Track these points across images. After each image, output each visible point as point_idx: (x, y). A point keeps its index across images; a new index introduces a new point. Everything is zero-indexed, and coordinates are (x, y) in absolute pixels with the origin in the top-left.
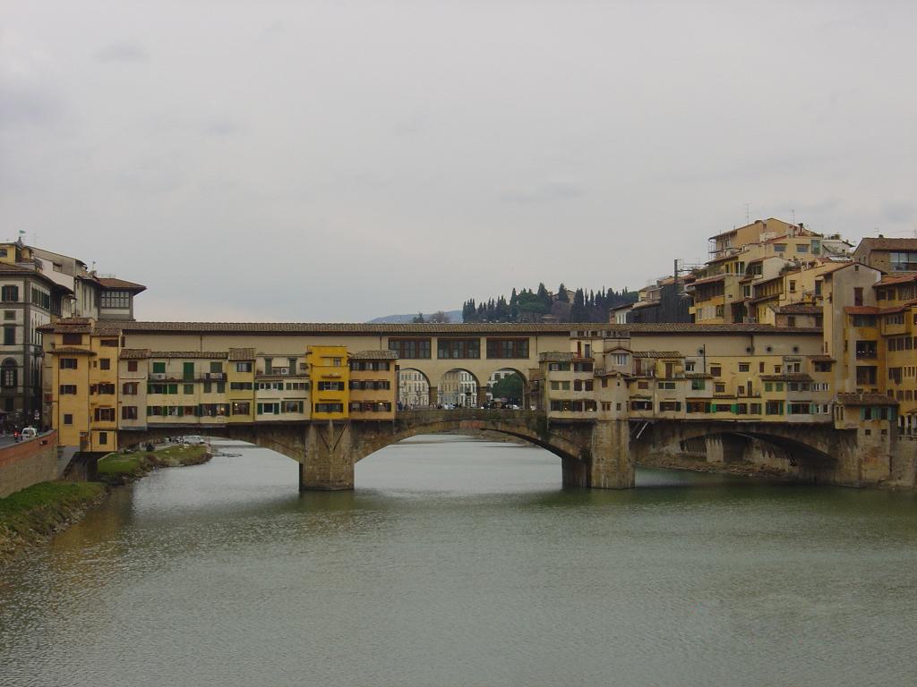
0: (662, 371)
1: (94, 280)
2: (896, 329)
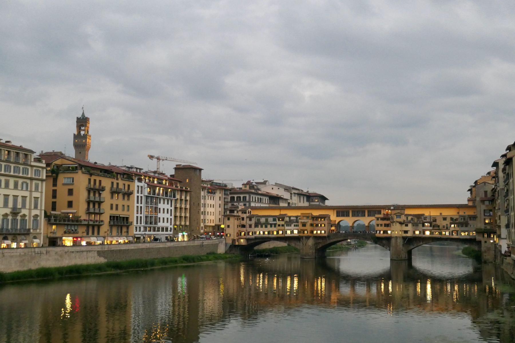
0: (416, 220)
1: (307, 194)
2: (494, 207)
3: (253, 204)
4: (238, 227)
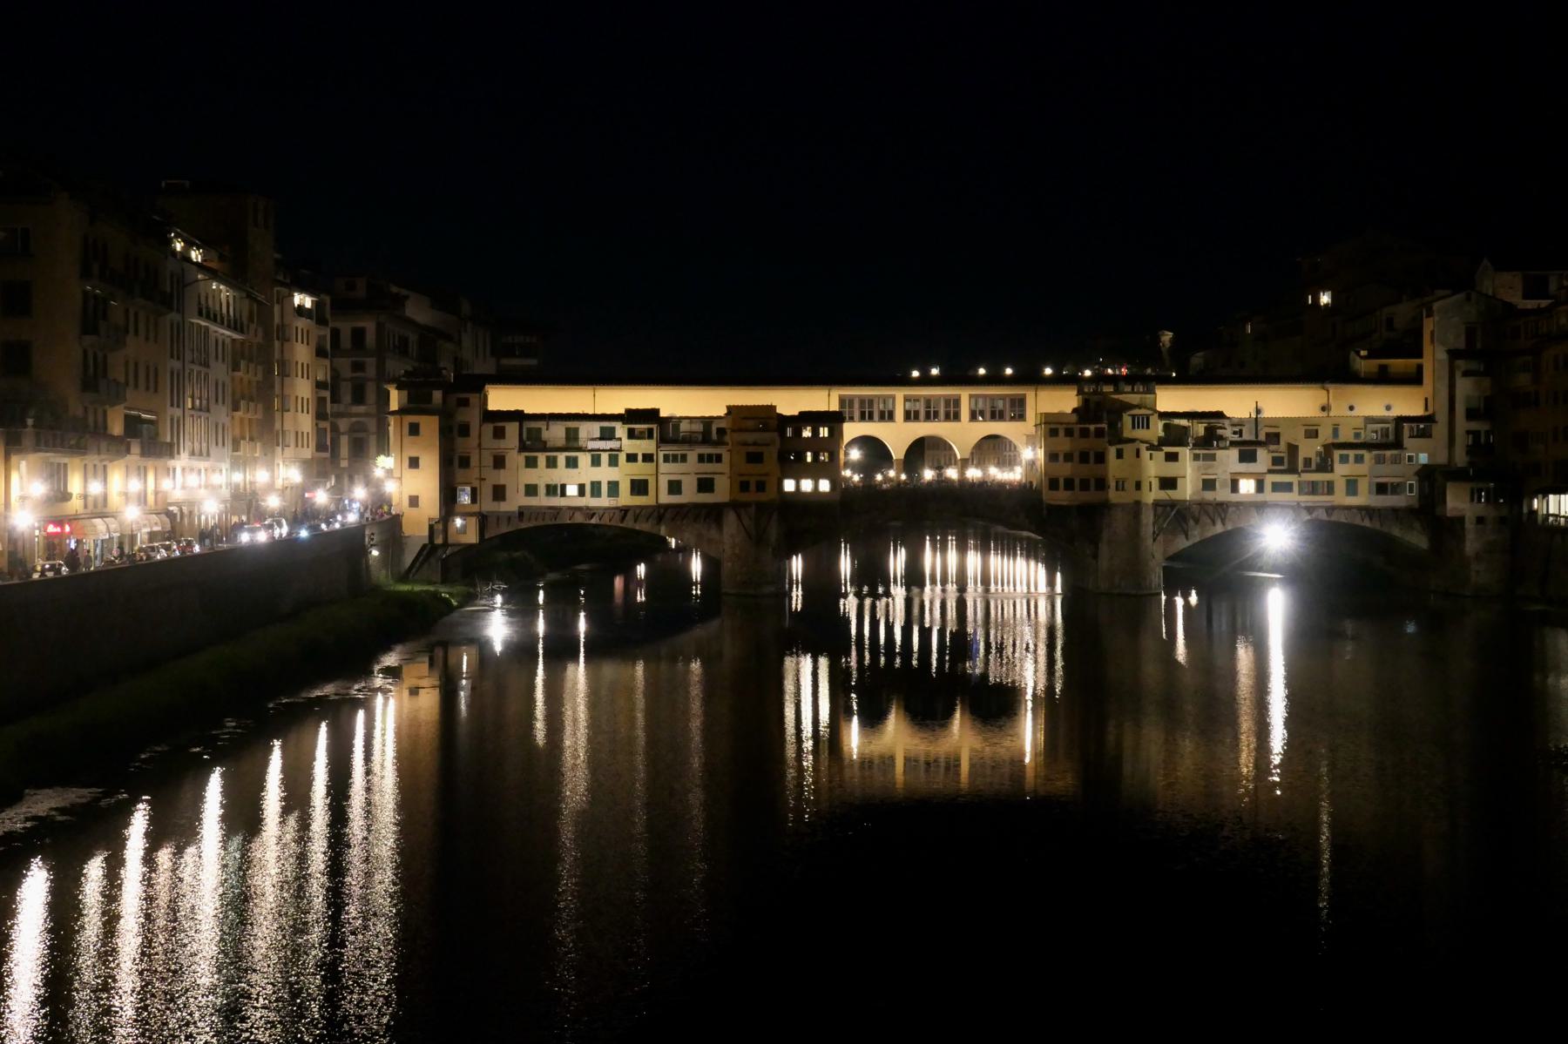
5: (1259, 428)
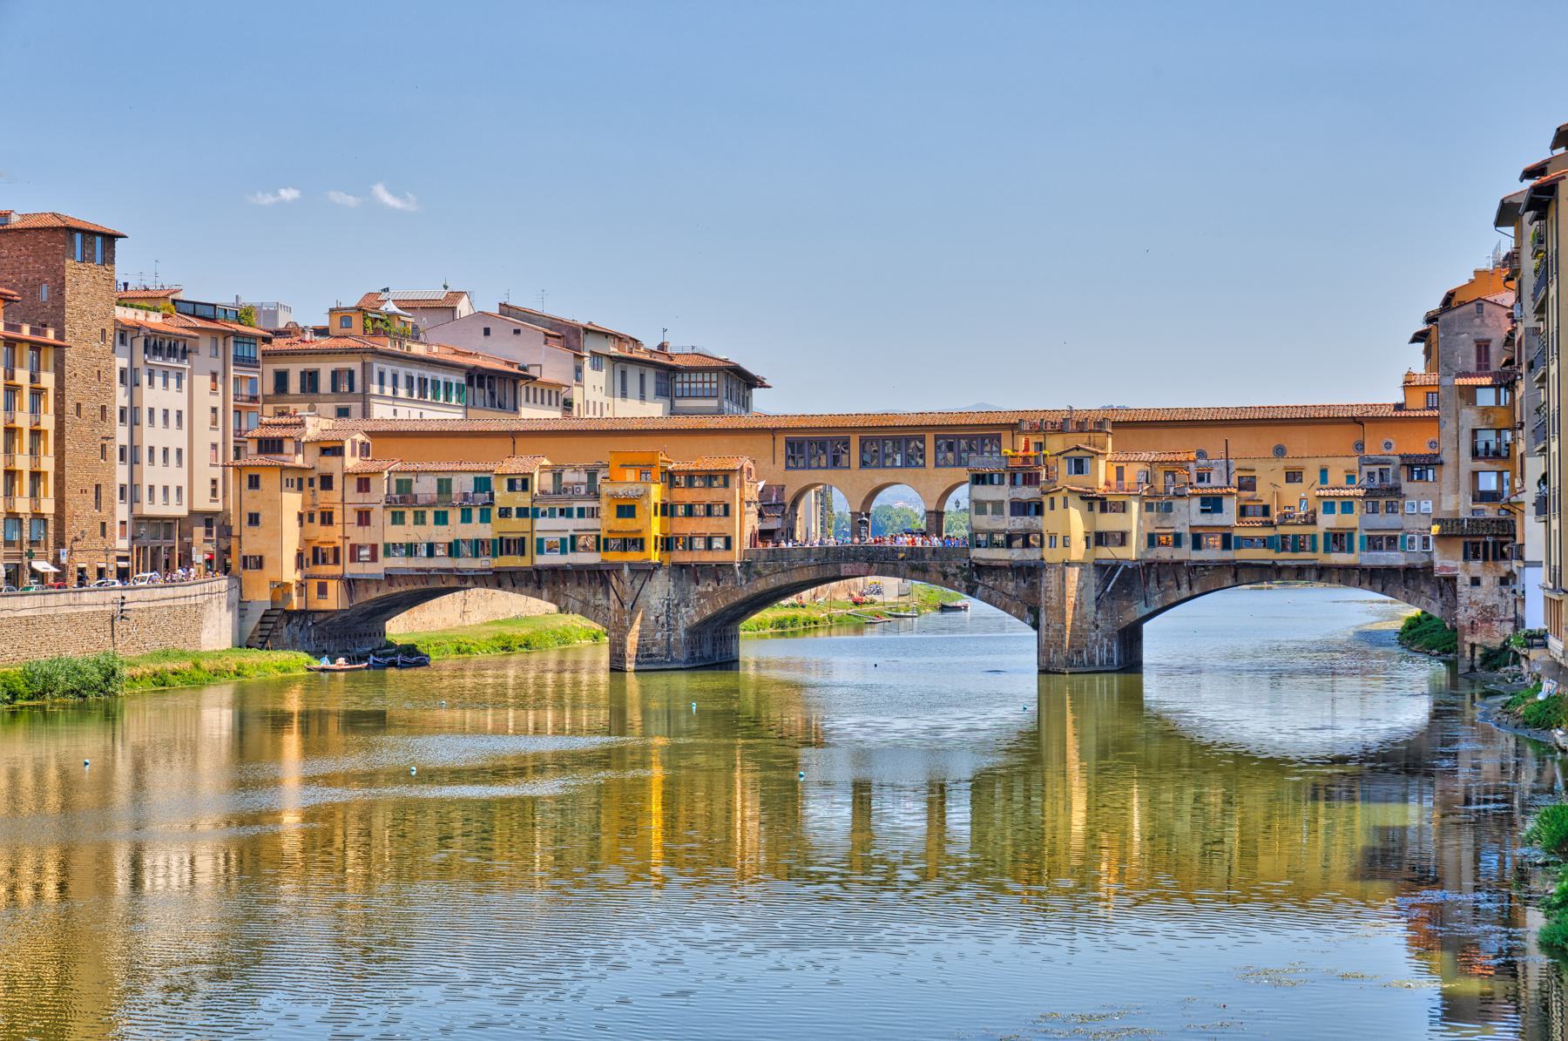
3: (381, 411)
4: (301, 525)
5: (1231, 471)
